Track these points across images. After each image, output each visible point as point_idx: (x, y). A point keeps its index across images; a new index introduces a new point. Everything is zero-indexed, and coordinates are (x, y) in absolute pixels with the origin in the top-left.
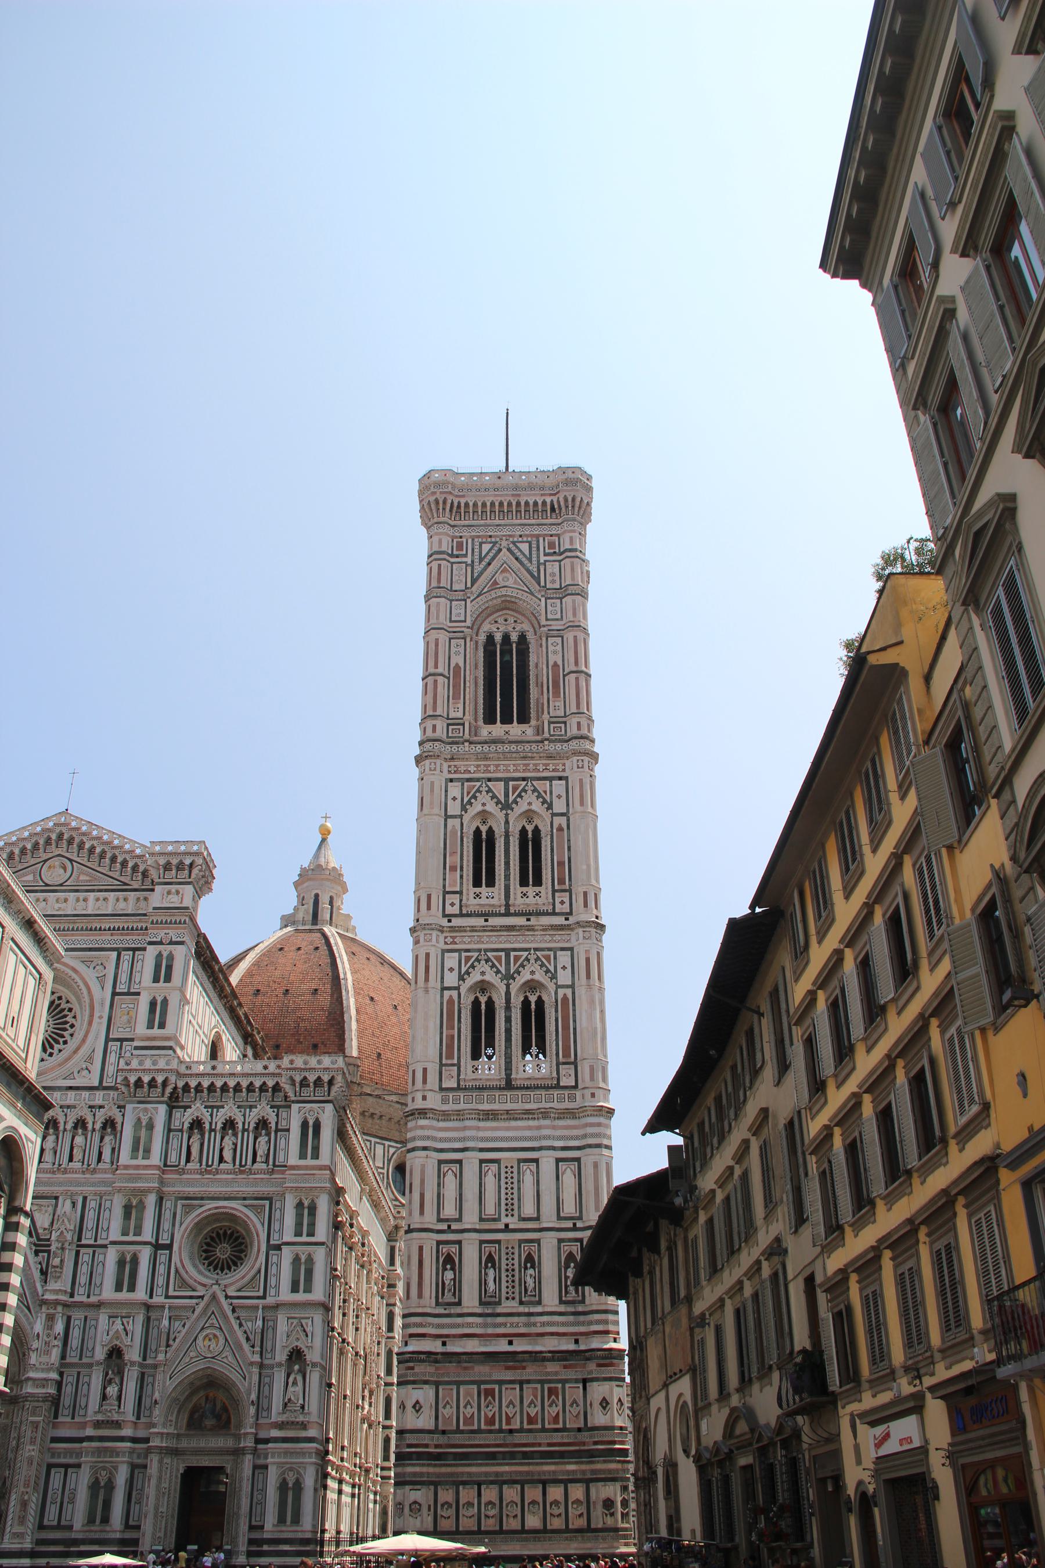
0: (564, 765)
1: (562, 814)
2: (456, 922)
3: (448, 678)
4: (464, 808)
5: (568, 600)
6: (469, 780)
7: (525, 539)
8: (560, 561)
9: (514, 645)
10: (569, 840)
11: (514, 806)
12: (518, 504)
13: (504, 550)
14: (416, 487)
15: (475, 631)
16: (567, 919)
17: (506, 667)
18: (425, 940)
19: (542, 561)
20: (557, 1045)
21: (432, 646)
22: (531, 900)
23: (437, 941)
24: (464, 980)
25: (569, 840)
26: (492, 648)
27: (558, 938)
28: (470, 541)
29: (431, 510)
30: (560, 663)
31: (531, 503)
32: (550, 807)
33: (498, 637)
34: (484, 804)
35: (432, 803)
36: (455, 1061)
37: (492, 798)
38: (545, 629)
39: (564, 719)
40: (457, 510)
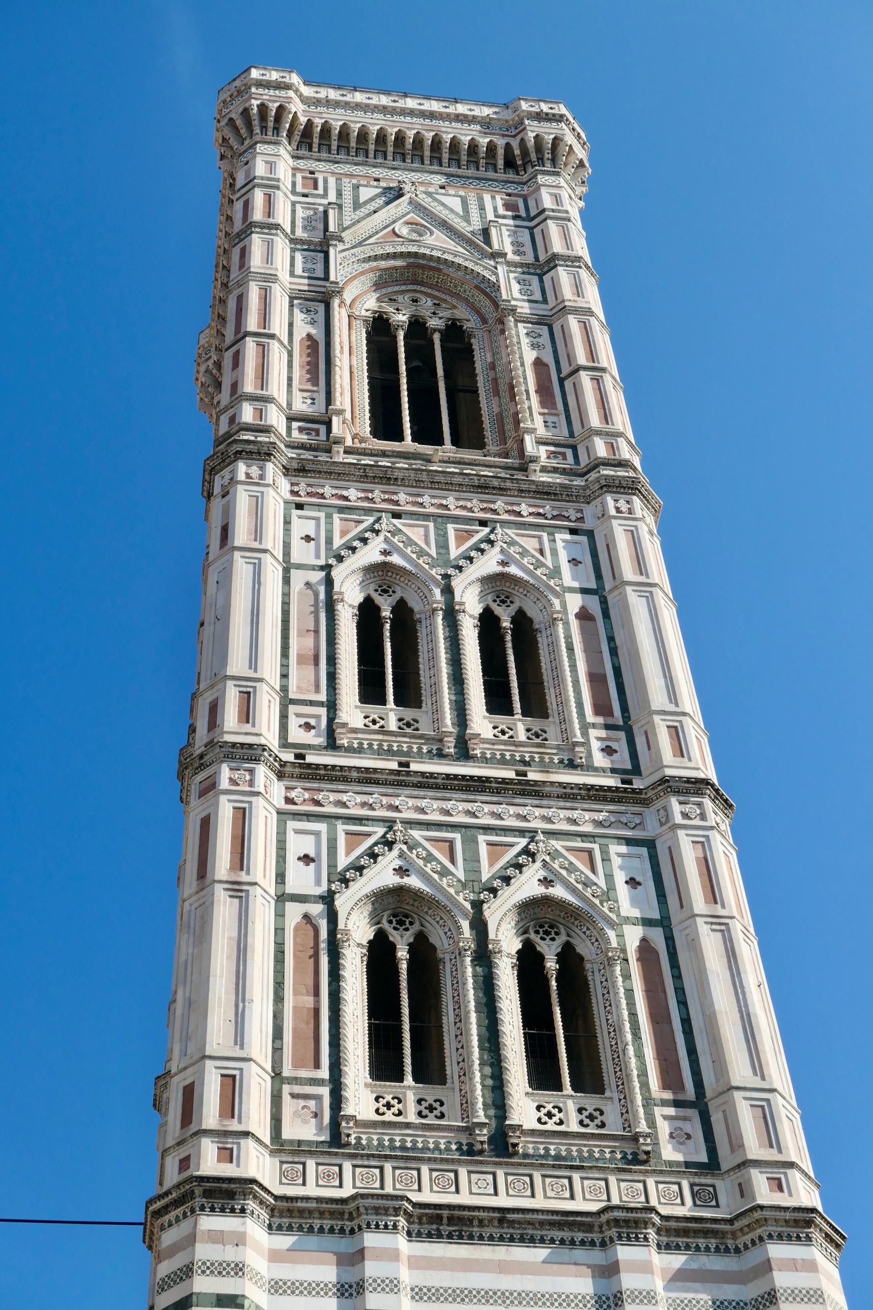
0: (581, 511)
3: (290, 354)
9: (437, 337)
10: (611, 639)
12: (437, 143)
18: (233, 781)
20: (640, 1056)
24: (345, 882)
25: (611, 639)
28: (332, 181)
36: (324, 1073)
39: (571, 441)
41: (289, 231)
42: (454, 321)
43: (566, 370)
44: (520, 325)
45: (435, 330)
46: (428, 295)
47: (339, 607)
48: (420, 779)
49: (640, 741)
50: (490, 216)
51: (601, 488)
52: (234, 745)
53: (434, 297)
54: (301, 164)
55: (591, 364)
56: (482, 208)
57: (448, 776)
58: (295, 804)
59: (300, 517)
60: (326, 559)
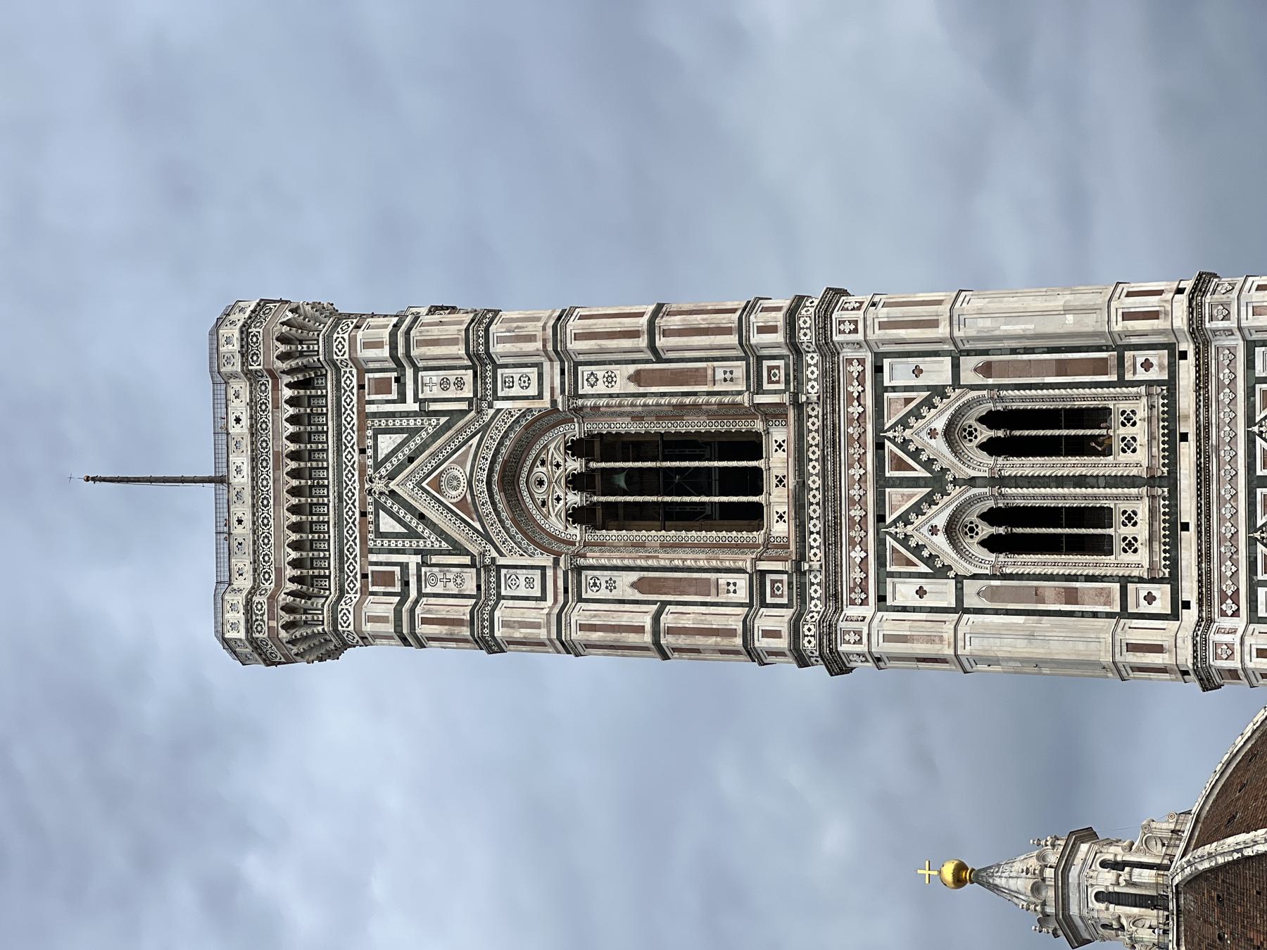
0: (850, 362)
1: (956, 367)
2: (1189, 591)
3: (665, 604)
4: (941, 572)
5: (497, 349)
7: (370, 442)
8: (417, 370)
9: (593, 465)
10: (1014, 351)
11: (937, 468)
12: (294, 456)
13: (392, 485)
14: (258, 669)
15: (564, 548)
16: (1183, 355)
17: (638, 481)
19: (416, 407)
21: (595, 636)
22: (1140, 432)
23: (1235, 632)
25: (1014, 351)
26: (599, 513)
27: (1225, 375)
28: (373, 558)
29: (305, 638)
30: (631, 369)
31: (291, 429)
32: (939, 391)
33: (575, 499)
34: (934, 530)
35: (930, 639)
37: (920, 512)
38: (560, 399)
42: (566, 448)
43: (649, 355)
44: (580, 392)
45: (586, 466)
47: (1008, 571)
49: (1134, 340)
52: (1195, 658)
58: (1238, 609)
59: (894, 598)
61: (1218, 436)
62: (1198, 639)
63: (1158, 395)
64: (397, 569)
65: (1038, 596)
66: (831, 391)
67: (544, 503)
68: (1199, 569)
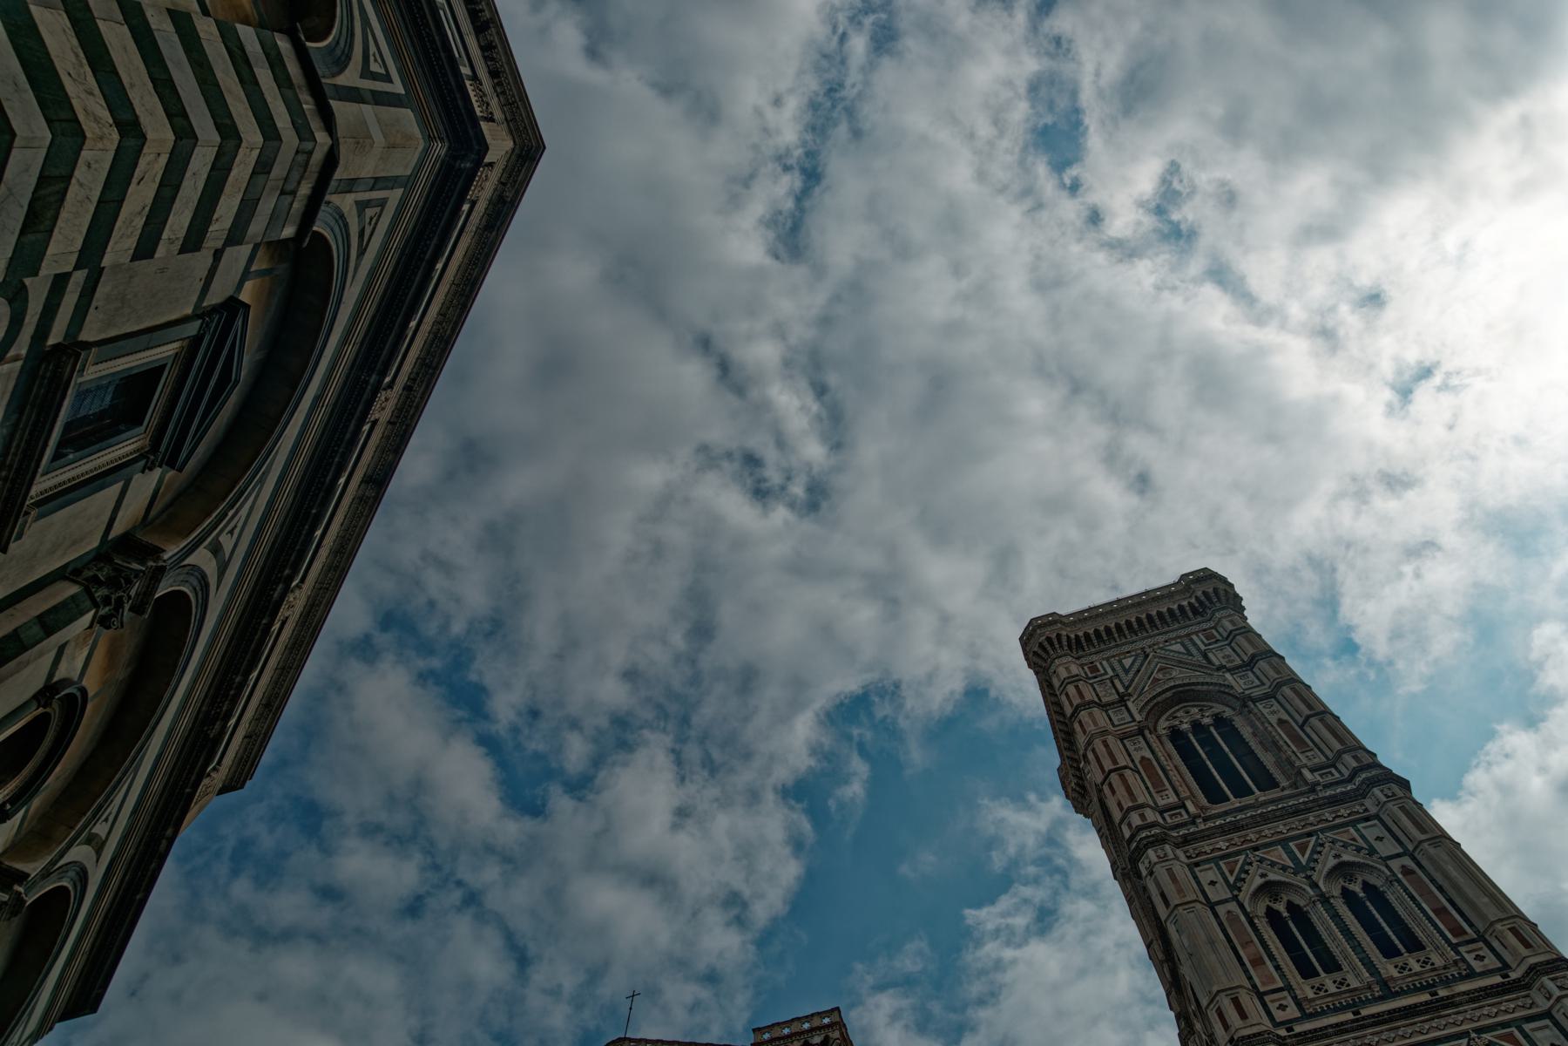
0: (1363, 805)
1: (1398, 856)
4: (1232, 887)
5: (1262, 664)
6: (1223, 857)
8: (1229, 644)
9: (1212, 729)
10: (1433, 881)
11: (1312, 865)
25: (1433, 881)
28: (1104, 663)
30: (1286, 717)
31: (1164, 610)
32: (1372, 852)
34: (1263, 876)
35: (1180, 891)
40: (1077, 645)
41: (1098, 701)
43: (1300, 721)
44: (1257, 704)
45: (1209, 726)
46: (1193, 706)
47: (1256, 921)
48: (1373, 1020)
49: (1495, 944)
50: (1203, 648)
51: (1368, 786)
52: (1249, 1037)
53: (1196, 706)
54: (1083, 661)
55: (1312, 712)
56: (1195, 644)
57: (1389, 1012)
59: (1201, 871)
60: (1231, 892)
61: (1449, 1015)
62: (1266, 1036)
63: (1460, 969)
64: (1103, 672)
65: (1246, 944)
66: (1334, 801)
67: (1176, 717)
68: (1326, 1028)
